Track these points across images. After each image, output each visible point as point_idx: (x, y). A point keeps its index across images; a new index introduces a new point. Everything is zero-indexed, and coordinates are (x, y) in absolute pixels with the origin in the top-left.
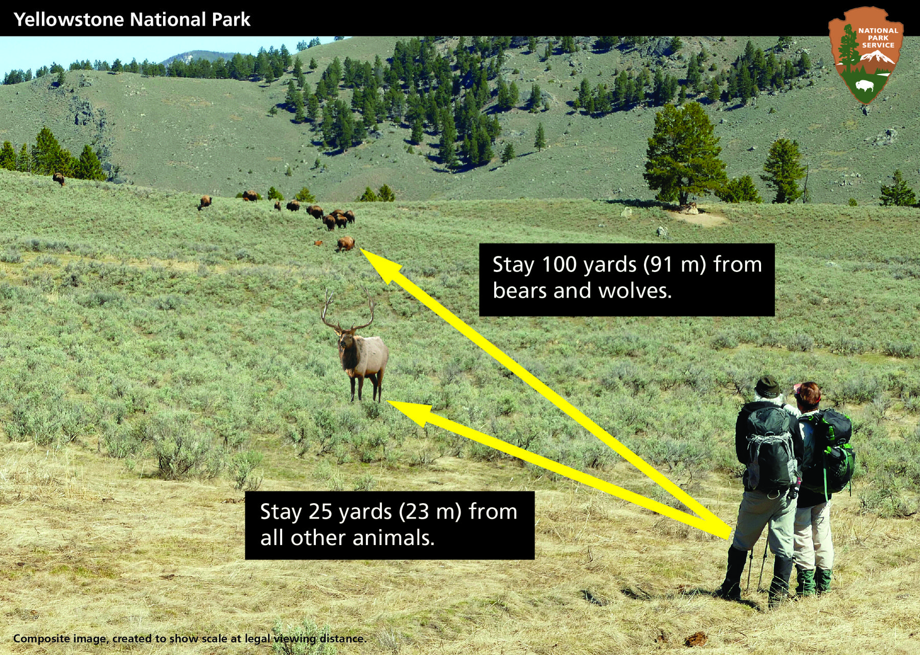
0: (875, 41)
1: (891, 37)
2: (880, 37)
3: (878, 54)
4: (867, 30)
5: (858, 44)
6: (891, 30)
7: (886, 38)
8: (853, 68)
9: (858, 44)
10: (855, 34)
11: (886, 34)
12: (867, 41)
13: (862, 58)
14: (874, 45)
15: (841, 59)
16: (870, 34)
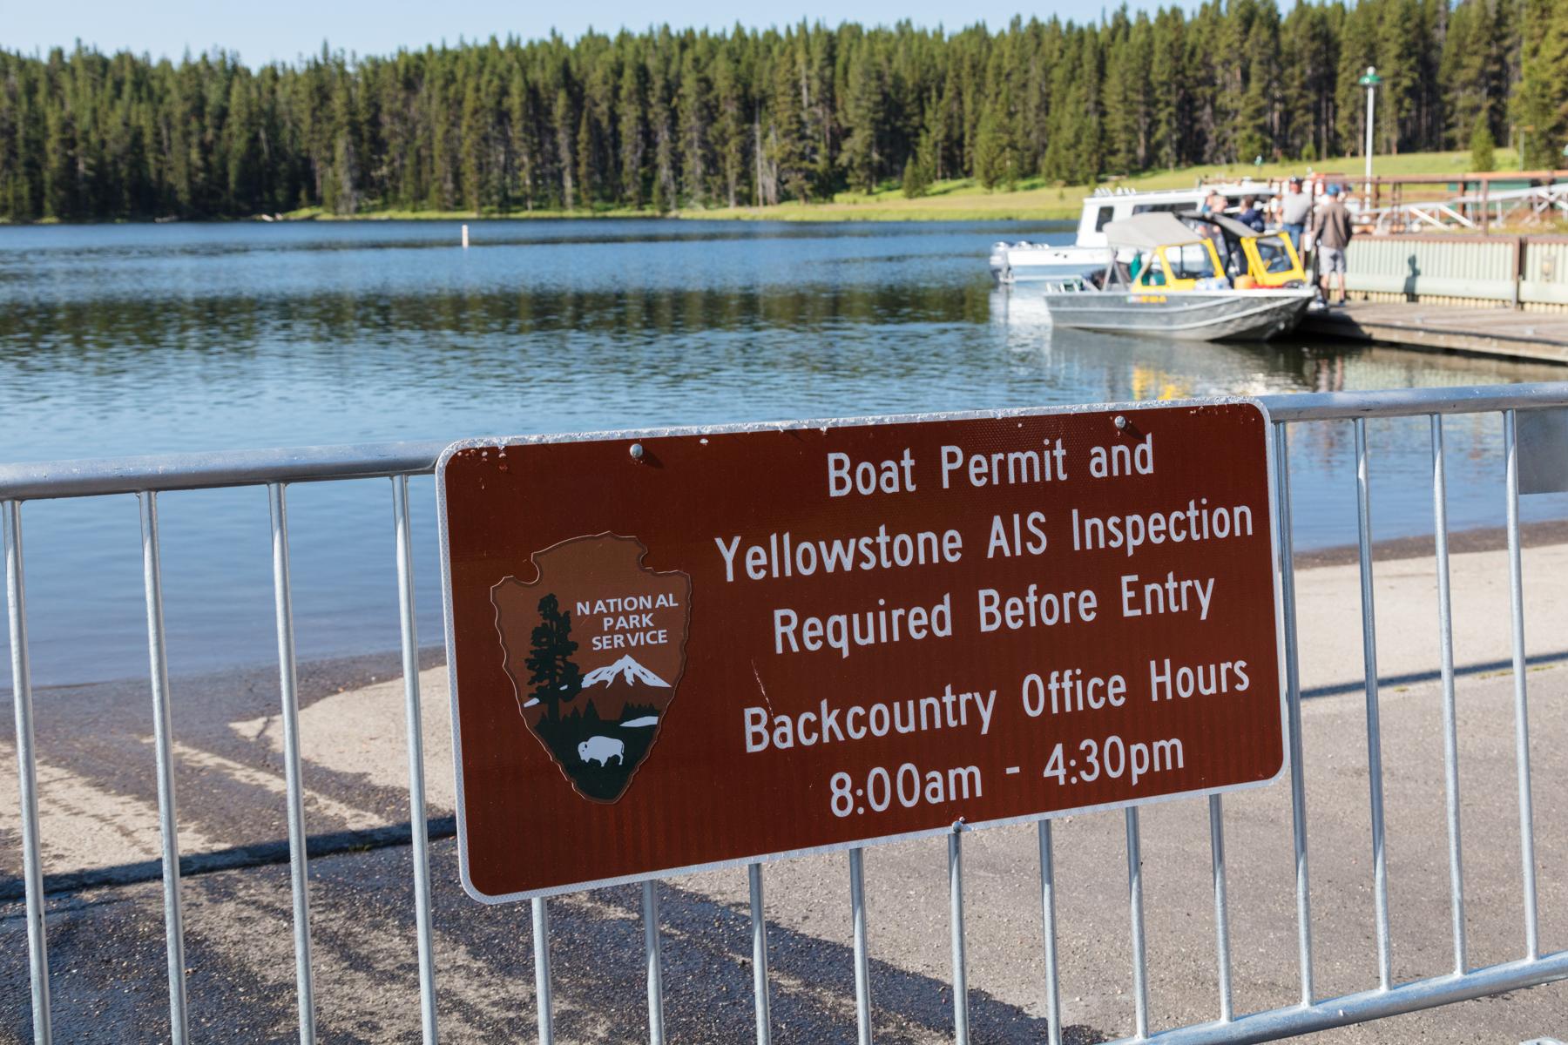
0: (623, 631)
1: (661, 617)
2: (634, 621)
3: (629, 667)
5: (575, 646)
6: (662, 600)
7: (646, 620)
8: (565, 709)
9: (575, 646)
10: (566, 620)
11: (646, 611)
12: (602, 633)
13: (588, 681)
14: (618, 640)
15: (533, 688)
16: (609, 614)
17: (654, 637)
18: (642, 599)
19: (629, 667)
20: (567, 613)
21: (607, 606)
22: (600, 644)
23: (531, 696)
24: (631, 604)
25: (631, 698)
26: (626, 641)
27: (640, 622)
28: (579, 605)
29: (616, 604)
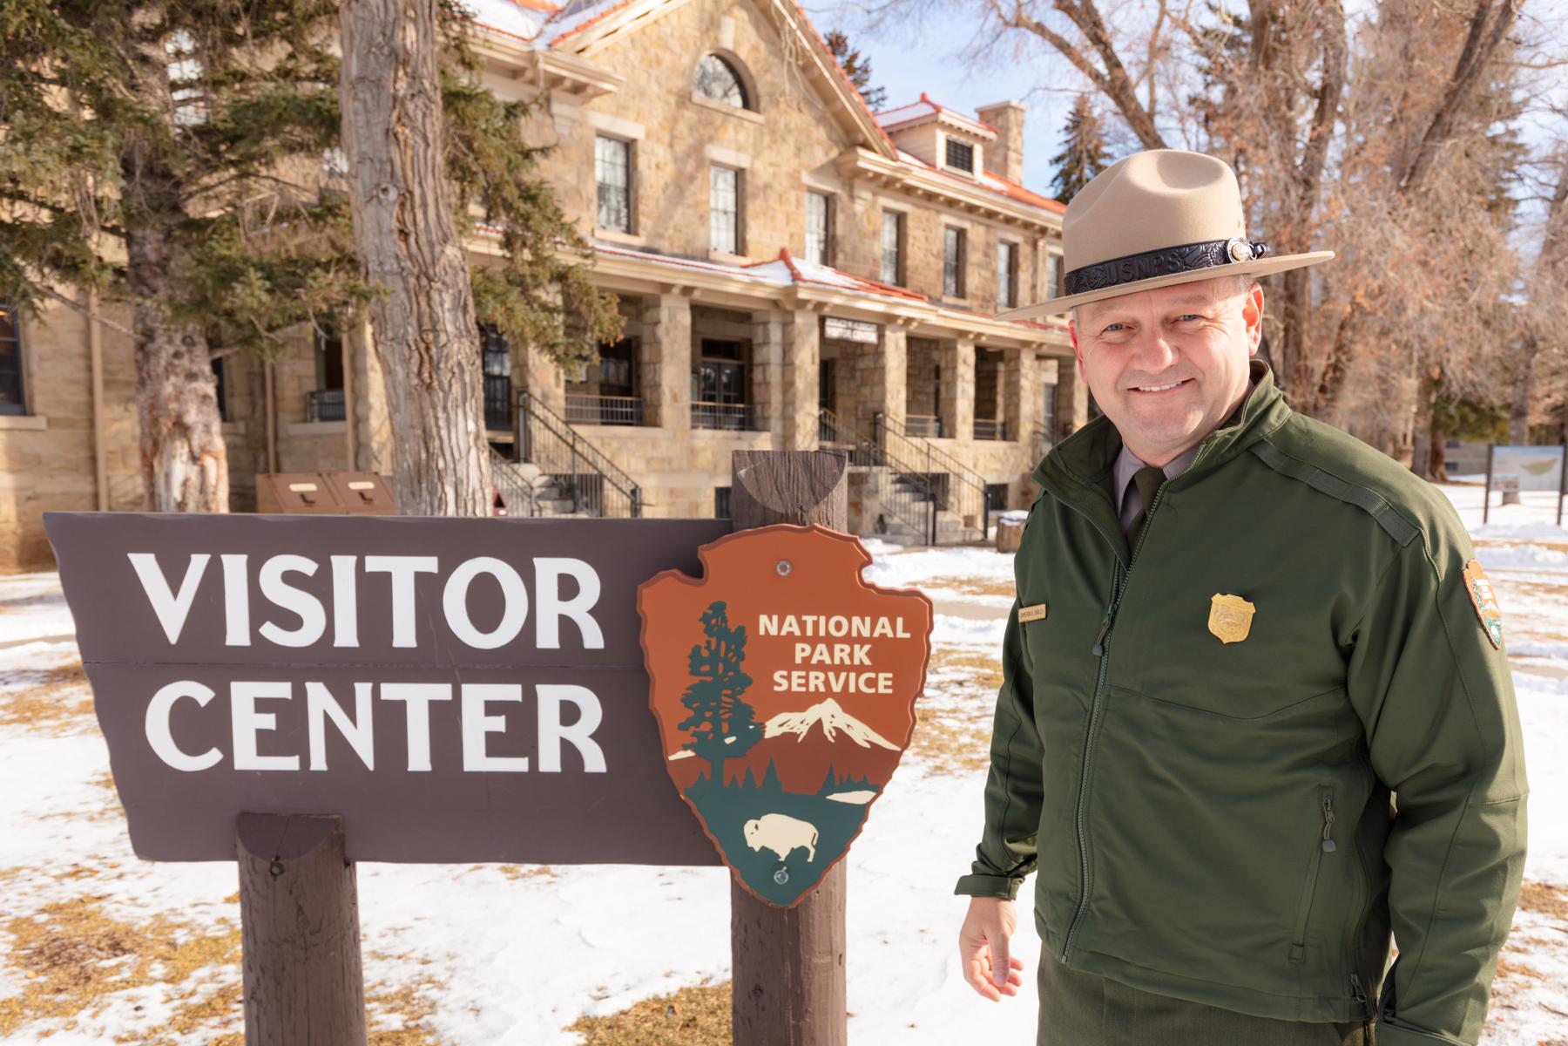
0: (821, 666)
2: (841, 653)
3: (831, 715)
4: (791, 625)
6: (884, 627)
7: (861, 654)
11: (861, 640)
12: (791, 666)
14: (816, 681)
16: (803, 638)
17: (871, 683)
18: (856, 620)
20: (741, 630)
21: (802, 625)
24: (838, 626)
26: (827, 682)
27: (851, 655)
28: (763, 619)
29: (816, 624)
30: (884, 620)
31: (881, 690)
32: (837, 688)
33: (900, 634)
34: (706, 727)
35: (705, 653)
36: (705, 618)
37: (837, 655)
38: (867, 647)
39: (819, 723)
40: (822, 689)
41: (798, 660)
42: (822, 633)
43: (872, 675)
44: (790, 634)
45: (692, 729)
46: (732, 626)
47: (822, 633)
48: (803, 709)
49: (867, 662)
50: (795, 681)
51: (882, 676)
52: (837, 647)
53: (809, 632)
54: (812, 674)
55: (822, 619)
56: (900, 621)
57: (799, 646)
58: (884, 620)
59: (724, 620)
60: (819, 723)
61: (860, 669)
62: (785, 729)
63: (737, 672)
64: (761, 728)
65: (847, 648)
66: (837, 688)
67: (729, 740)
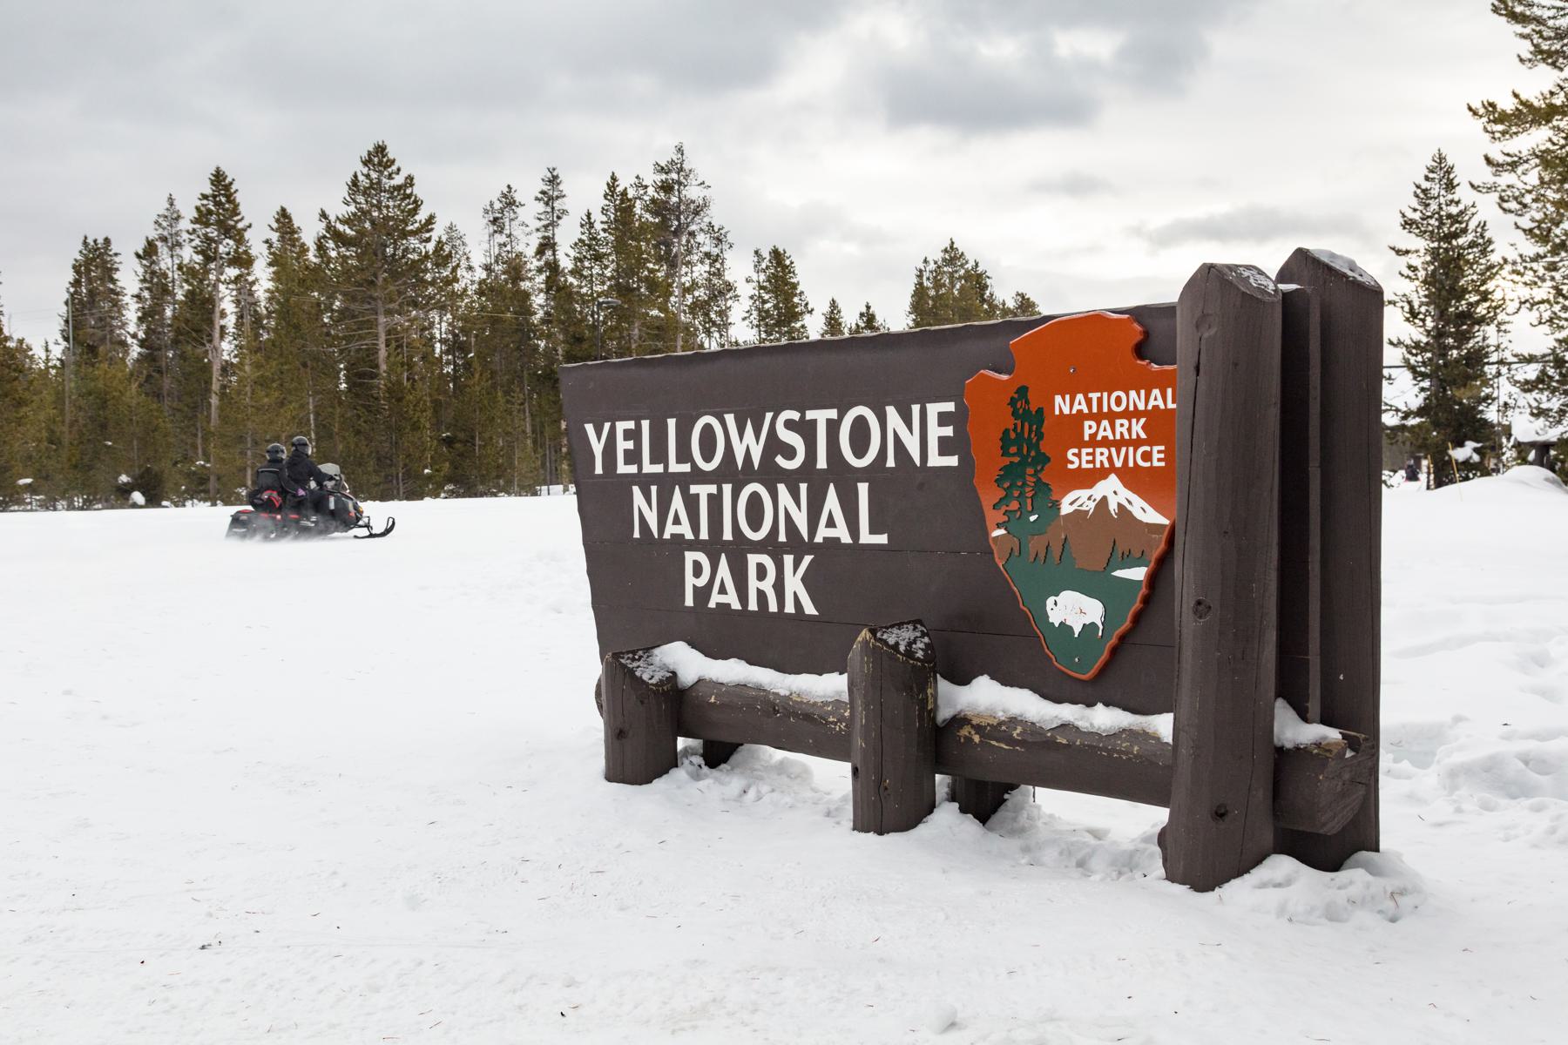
0: (1105, 442)
1: (1157, 424)
2: (1122, 427)
3: (1112, 490)
4: (1080, 404)
6: (1156, 399)
7: (1138, 428)
11: (1137, 414)
12: (1081, 444)
13: (1066, 508)
16: (1091, 416)
17: (1147, 456)
18: (1133, 394)
19: (1112, 490)
20: (1040, 411)
21: (1089, 402)
22: (1077, 459)
23: (999, 526)
24: (1118, 401)
25: (1112, 530)
26: (1110, 459)
27: (1129, 430)
29: (1100, 400)
30: (1156, 392)
31: (1156, 464)
32: (1118, 464)
33: (1171, 406)
34: (1014, 505)
35: (1013, 435)
36: (1013, 402)
37: (1118, 429)
38: (1143, 420)
39: (1104, 501)
40: (1107, 465)
41: (1087, 438)
42: (1105, 409)
43: (1147, 448)
44: (1080, 411)
45: (1004, 508)
46: (1033, 409)
47: (1105, 409)
48: (1090, 486)
49: (1143, 436)
50: (1085, 458)
51: (1156, 448)
52: (1118, 422)
53: (1095, 410)
54: (1098, 450)
55: (1105, 395)
56: (1169, 391)
57: (1087, 423)
58: (1156, 392)
59: (1027, 402)
60: (1104, 499)
61: (1137, 443)
62: (1075, 507)
63: (1038, 451)
64: (1056, 505)
65: (1126, 422)
66: (1118, 464)
67: (1032, 518)
